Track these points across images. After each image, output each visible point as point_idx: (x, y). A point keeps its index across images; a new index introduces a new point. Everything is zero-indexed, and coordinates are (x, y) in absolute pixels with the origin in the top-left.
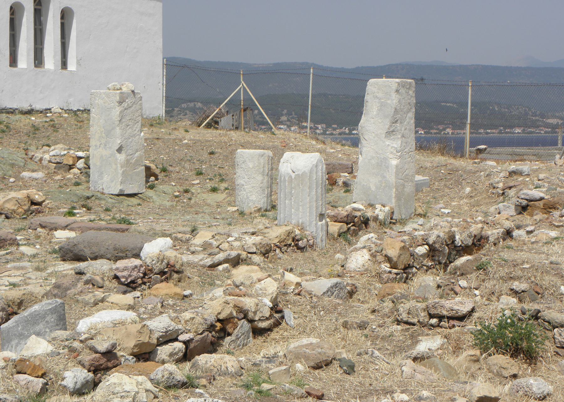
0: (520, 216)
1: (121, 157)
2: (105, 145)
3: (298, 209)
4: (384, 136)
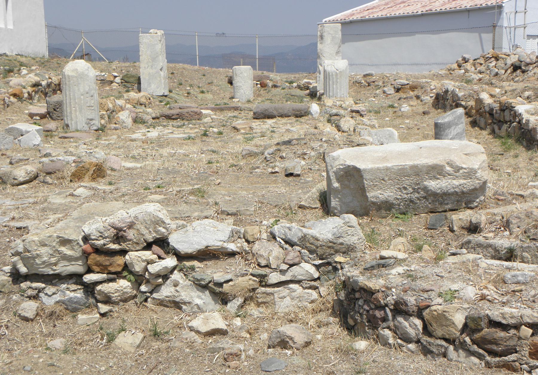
0: (397, 94)
1: (162, 73)
2: (152, 67)
3: (341, 90)
4: (335, 54)
